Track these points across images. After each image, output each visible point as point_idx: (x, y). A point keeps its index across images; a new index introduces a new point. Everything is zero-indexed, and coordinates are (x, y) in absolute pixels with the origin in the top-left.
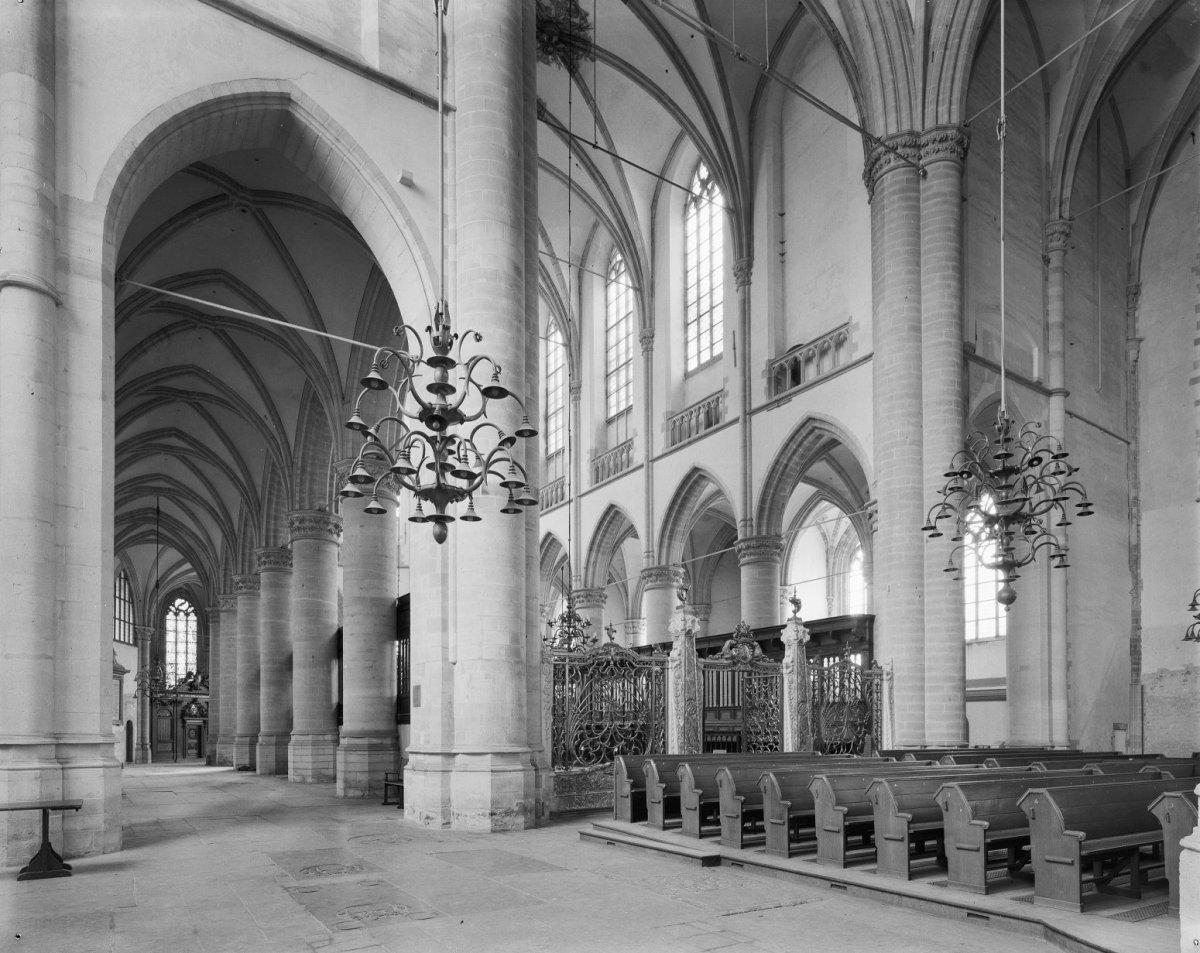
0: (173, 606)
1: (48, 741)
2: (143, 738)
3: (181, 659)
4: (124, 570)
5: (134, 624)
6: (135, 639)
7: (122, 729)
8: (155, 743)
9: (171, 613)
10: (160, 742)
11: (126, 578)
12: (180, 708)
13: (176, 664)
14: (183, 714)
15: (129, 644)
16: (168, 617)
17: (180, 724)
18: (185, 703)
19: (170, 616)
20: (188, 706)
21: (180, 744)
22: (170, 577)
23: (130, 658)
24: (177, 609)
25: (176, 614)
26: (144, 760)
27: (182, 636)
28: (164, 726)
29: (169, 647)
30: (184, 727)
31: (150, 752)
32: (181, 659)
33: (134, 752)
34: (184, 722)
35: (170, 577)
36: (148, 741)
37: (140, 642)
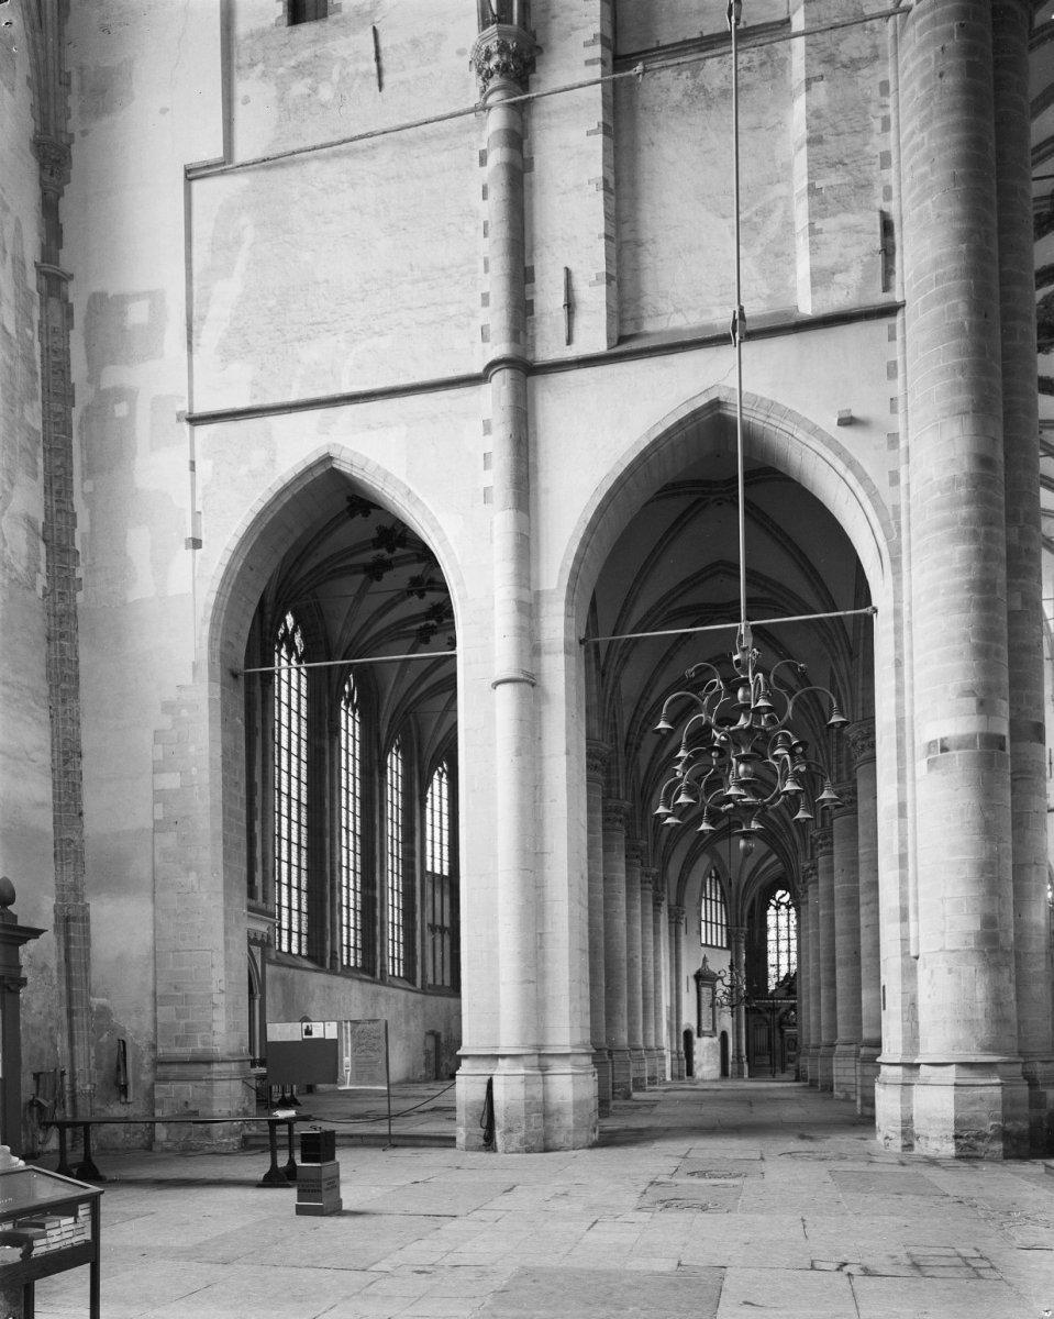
0: (774, 899)
1: (531, 1051)
2: (738, 1049)
3: (784, 960)
4: (715, 868)
5: (727, 925)
6: (728, 942)
7: (716, 1040)
8: (752, 1055)
9: (772, 908)
10: (756, 1054)
11: (717, 877)
12: (777, 1016)
13: (778, 965)
14: (781, 1023)
15: (722, 948)
16: (769, 912)
17: (778, 1034)
18: (783, 1010)
19: (771, 911)
20: (786, 1013)
21: (779, 1056)
22: (761, 870)
23: (720, 963)
24: (778, 902)
25: (777, 908)
26: (740, 1074)
27: (784, 934)
28: (762, 1037)
29: (771, 946)
30: (782, 1037)
31: (746, 1066)
32: (784, 960)
33: (730, 1066)
34: (782, 1032)
35: (761, 870)
36: (744, 1052)
37: (733, 946)
